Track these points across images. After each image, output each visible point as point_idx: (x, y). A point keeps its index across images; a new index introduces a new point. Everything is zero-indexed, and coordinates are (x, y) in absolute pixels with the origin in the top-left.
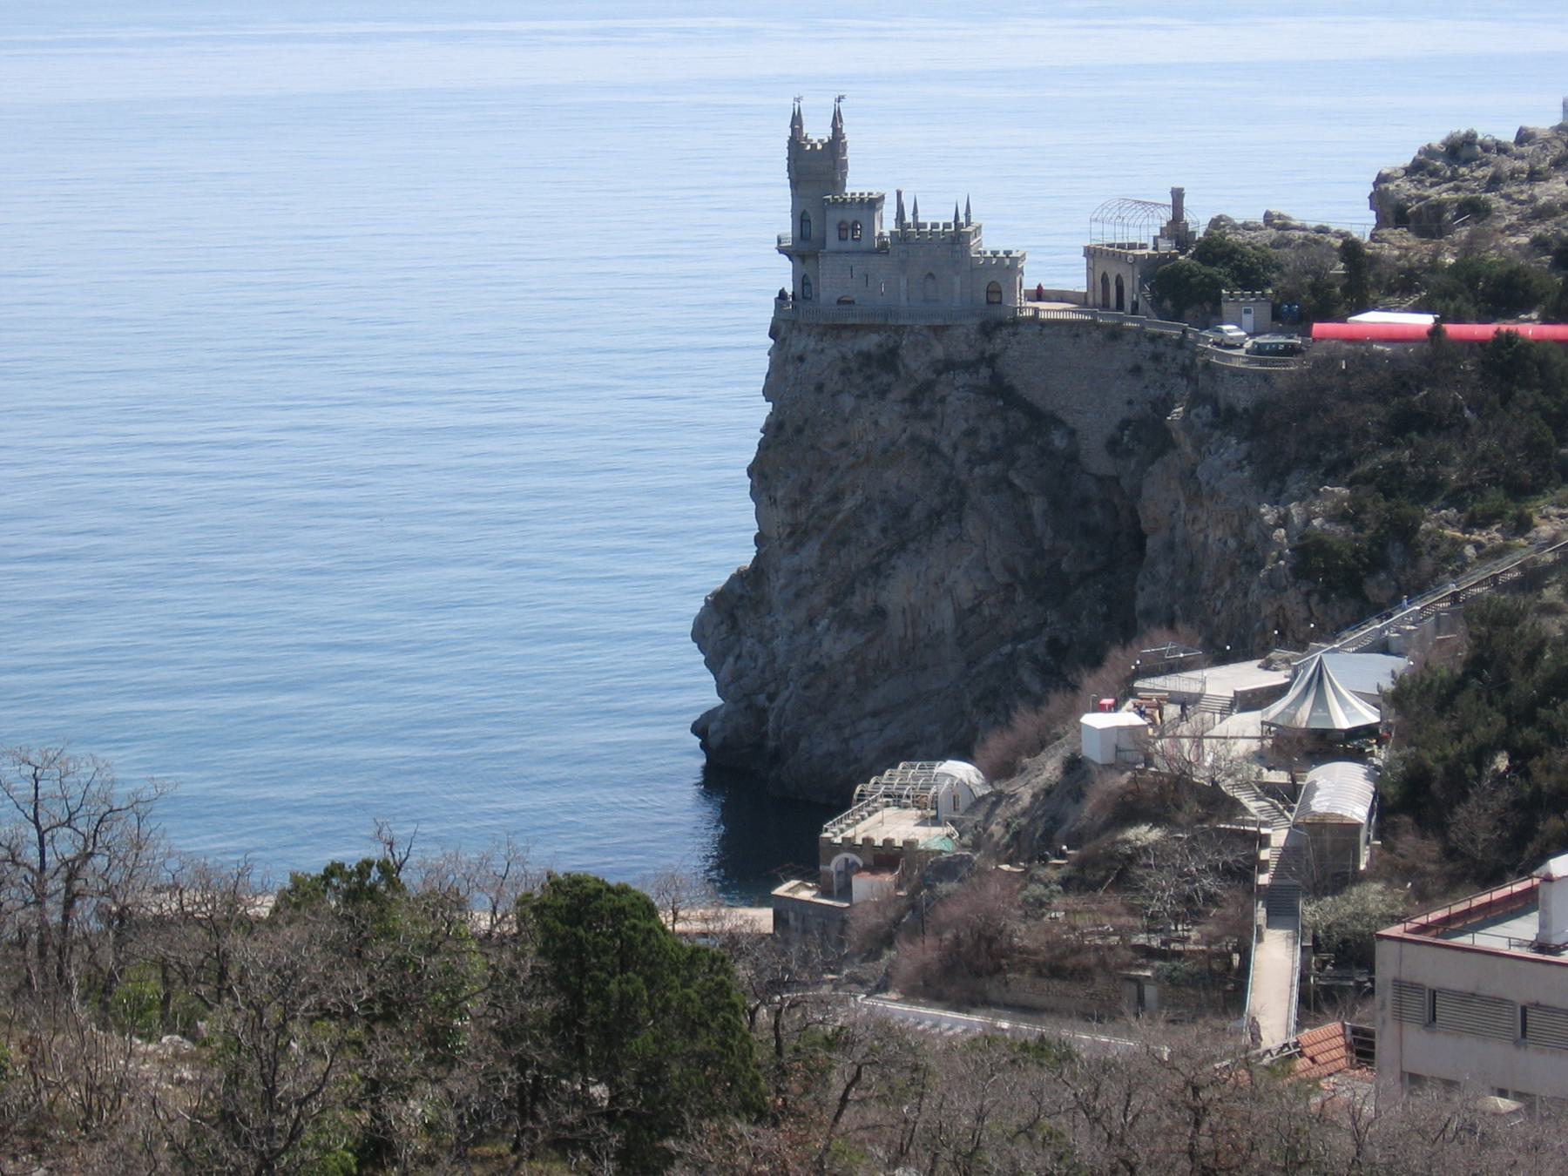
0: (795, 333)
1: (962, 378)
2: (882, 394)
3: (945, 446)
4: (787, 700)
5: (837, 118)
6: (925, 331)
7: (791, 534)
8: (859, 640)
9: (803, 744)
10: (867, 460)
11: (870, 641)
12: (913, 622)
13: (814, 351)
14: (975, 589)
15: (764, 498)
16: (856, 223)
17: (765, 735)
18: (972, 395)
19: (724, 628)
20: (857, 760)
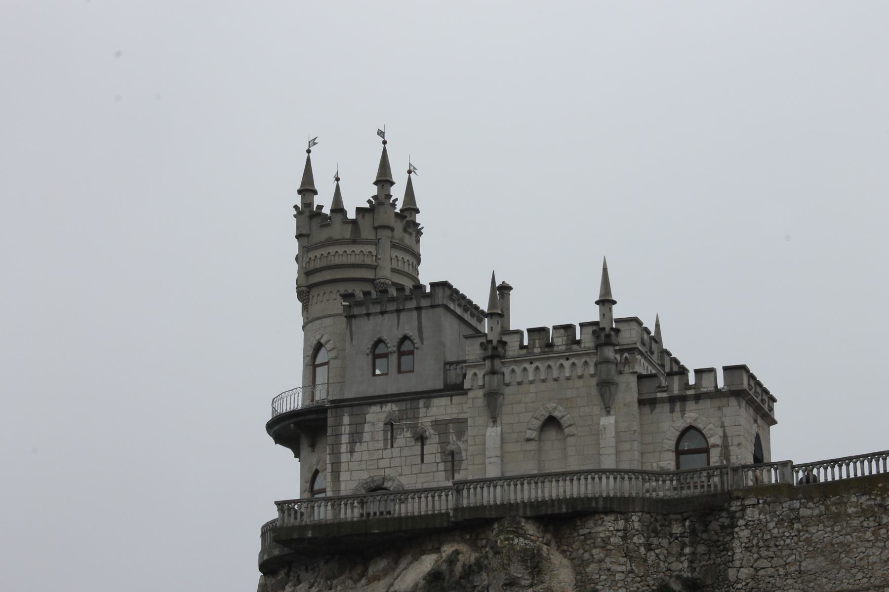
6: (531, 529)
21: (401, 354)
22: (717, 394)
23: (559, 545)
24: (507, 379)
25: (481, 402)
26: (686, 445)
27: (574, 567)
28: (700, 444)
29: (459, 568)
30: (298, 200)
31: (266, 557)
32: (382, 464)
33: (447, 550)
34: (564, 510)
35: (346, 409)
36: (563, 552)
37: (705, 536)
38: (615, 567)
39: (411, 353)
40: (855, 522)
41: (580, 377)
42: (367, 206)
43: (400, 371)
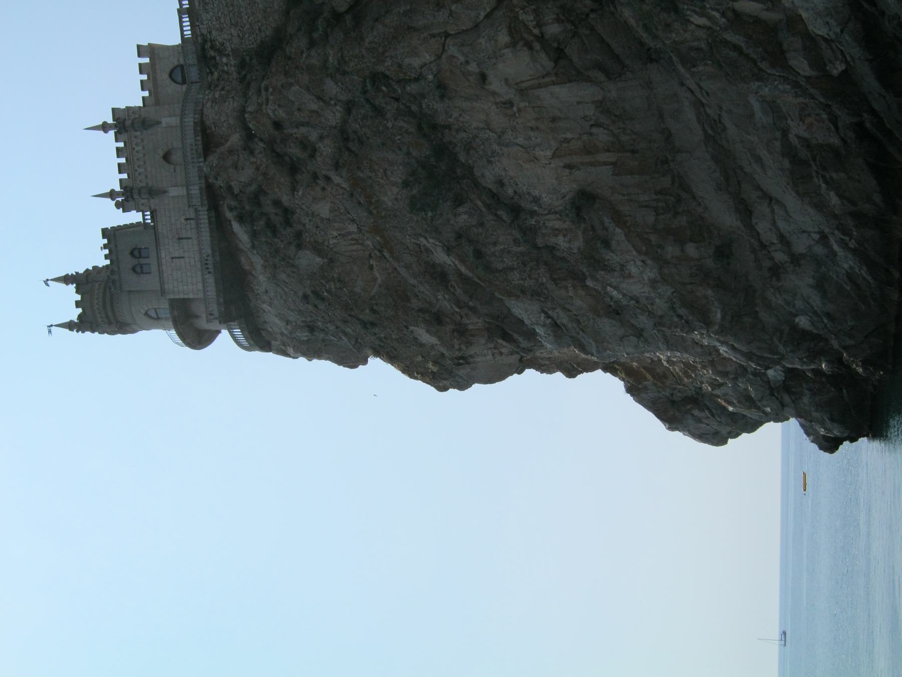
0: (270, 330)
2: (287, 213)
3: (333, 116)
4: (733, 348)
5: (57, 280)
6: (211, 158)
7: (506, 337)
8: (619, 234)
9: (803, 322)
10: (376, 230)
11: (618, 218)
12: (588, 150)
14: (513, 45)
15: (462, 372)
16: (132, 254)
17: (818, 372)
19: (696, 412)
20: (824, 238)
21: (140, 257)
24: (144, 184)
26: (179, 79)
28: (179, 68)
32: (192, 263)
33: (229, 215)
34: (199, 138)
35: (166, 287)
36: (226, 141)
37: (218, 58)
39: (140, 249)
41: (143, 141)
43: (148, 257)
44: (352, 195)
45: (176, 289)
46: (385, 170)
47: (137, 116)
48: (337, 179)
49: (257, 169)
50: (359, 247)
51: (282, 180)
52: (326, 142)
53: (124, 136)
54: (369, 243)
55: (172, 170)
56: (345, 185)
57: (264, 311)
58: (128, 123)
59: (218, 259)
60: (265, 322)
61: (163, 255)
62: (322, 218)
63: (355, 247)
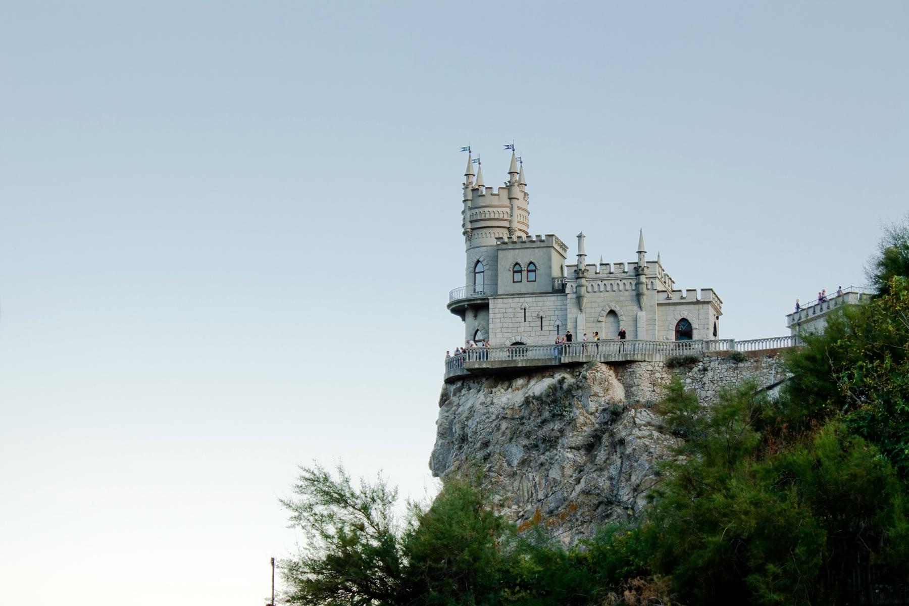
0: (463, 392)
1: (644, 416)
3: (625, 495)
6: (604, 368)
13: (482, 404)
18: (656, 434)
21: (528, 271)
22: (698, 302)
23: (617, 376)
24: (590, 289)
25: (574, 301)
27: (625, 387)
29: (565, 386)
30: (464, 180)
31: (451, 375)
32: (519, 330)
33: (558, 376)
34: (621, 359)
37: (690, 374)
38: (646, 389)
40: (765, 371)
42: (504, 186)
44: (565, 499)
45: (497, 311)
46: (583, 533)
47: (649, 287)
48: (578, 488)
49: (592, 414)
50: (526, 498)
51: (580, 438)
52: (608, 482)
53: (632, 273)
54: (529, 507)
55: (601, 319)
56: (574, 494)
57: (479, 391)
58: (643, 279)
59: (520, 365)
60: (470, 389)
61: (528, 300)
62: (547, 470)
63: (526, 494)
